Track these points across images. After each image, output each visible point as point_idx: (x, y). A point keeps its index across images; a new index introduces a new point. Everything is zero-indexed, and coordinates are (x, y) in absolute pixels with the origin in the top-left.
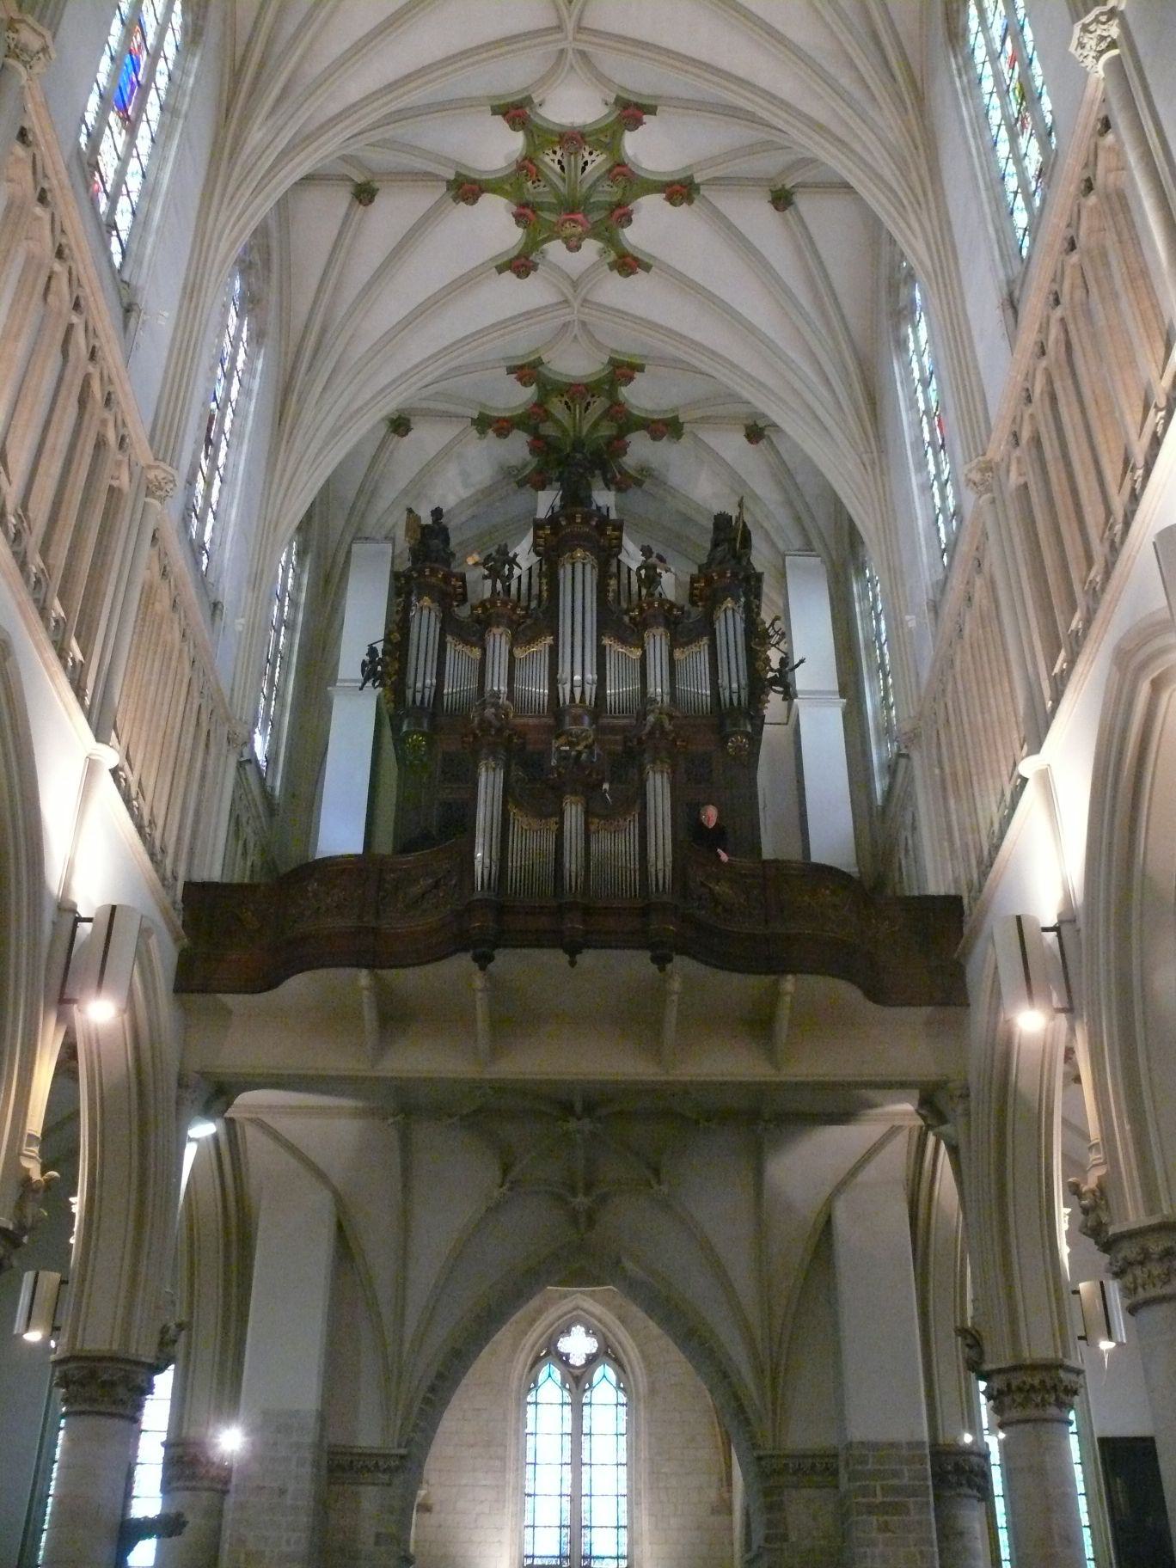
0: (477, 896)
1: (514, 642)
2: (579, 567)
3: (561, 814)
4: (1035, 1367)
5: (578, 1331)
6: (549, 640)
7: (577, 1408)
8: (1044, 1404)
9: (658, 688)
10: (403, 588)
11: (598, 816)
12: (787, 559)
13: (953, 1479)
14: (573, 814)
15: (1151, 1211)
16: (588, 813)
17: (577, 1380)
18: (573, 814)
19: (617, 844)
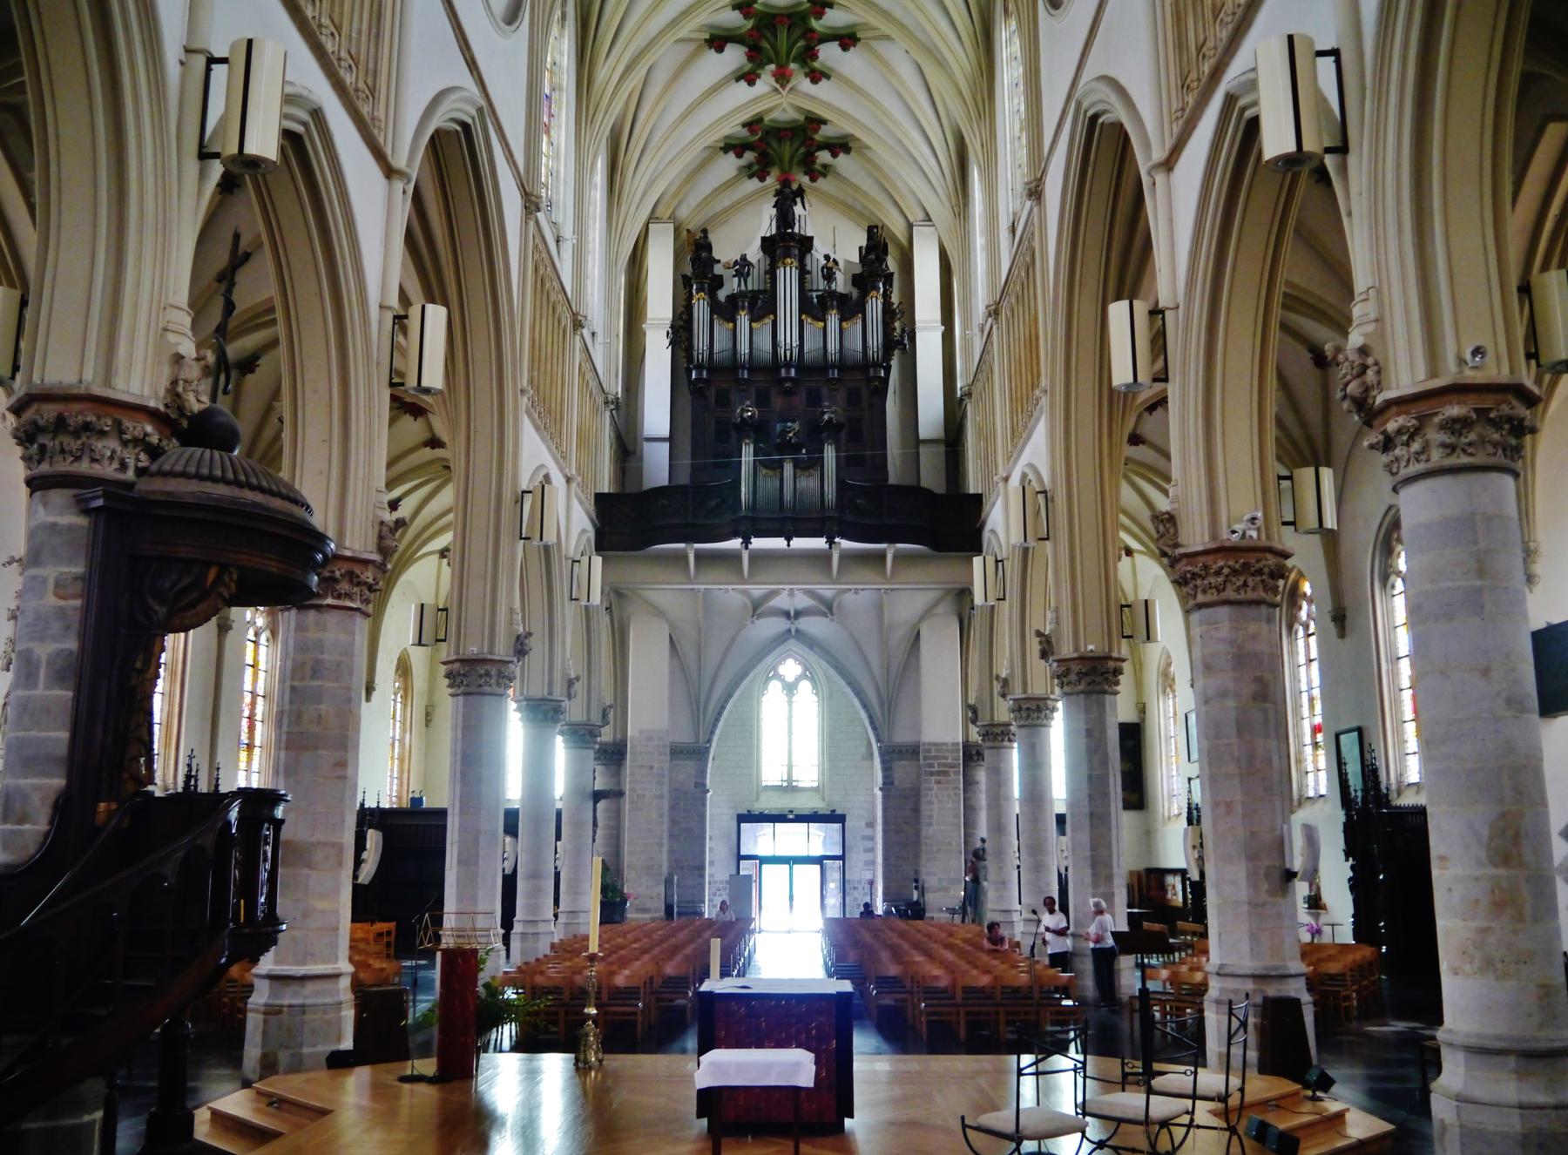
0: (743, 514)
1: (752, 321)
2: (788, 269)
3: (782, 468)
4: (999, 725)
5: (790, 662)
6: (772, 317)
7: (790, 703)
8: (1002, 740)
9: (833, 345)
10: (683, 284)
11: (802, 469)
12: (914, 228)
13: (975, 758)
14: (788, 469)
15: (1025, 692)
16: (795, 467)
17: (790, 688)
18: (788, 469)
19: (809, 483)
